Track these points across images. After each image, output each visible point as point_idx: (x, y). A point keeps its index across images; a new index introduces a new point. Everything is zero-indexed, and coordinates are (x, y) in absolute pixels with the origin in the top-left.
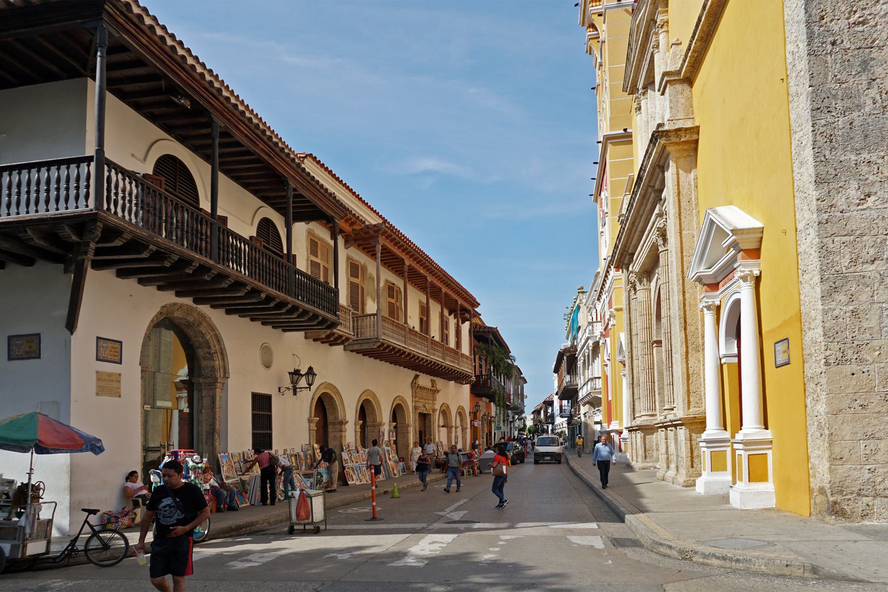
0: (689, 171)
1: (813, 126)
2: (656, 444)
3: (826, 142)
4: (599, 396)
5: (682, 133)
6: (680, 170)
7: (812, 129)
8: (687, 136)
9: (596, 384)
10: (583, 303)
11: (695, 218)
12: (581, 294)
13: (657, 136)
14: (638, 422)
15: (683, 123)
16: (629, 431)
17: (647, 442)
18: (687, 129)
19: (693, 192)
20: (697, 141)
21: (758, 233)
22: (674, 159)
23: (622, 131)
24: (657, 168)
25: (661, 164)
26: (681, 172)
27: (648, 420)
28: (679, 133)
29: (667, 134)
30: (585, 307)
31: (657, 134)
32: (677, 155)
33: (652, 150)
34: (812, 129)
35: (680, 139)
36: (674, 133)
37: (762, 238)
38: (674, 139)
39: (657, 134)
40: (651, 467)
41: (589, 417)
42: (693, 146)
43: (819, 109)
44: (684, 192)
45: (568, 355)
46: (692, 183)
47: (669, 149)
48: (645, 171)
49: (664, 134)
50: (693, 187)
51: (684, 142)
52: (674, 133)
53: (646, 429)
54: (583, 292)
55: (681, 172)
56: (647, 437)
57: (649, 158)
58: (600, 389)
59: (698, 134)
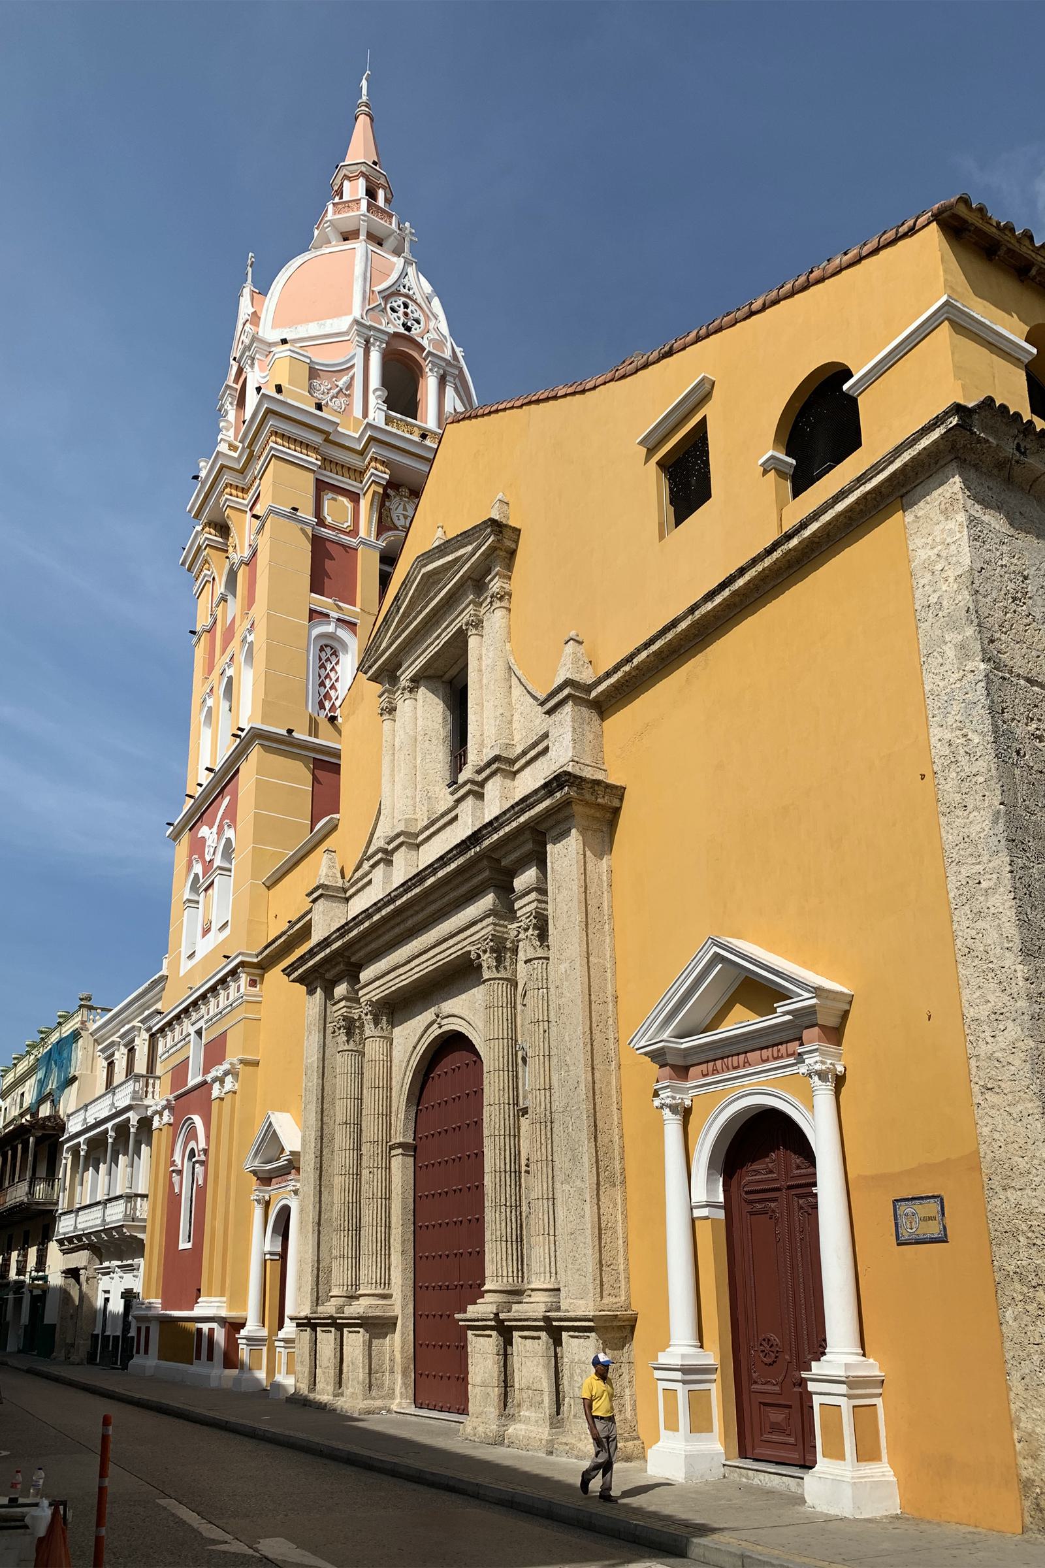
0: (600, 856)
1: (1010, 865)
2: (391, 1360)
3: (1025, 894)
4: (140, 1236)
6: (587, 849)
7: (1008, 868)
9: (135, 1209)
10: (87, 1030)
11: (608, 939)
12: (85, 1011)
13: (566, 781)
14: (328, 1309)
15: (592, 772)
16: (298, 1325)
17: (374, 1354)
19: (605, 893)
22: (580, 829)
24: (527, 832)
25: (541, 828)
26: (588, 853)
27: (377, 1306)
28: (596, 788)
30: (91, 1039)
32: (585, 824)
33: (540, 801)
34: (1008, 868)
35: (597, 798)
38: (588, 796)
39: (567, 778)
40: (381, 1409)
41: (88, 1279)
44: (592, 889)
45: (39, 1134)
46: (605, 878)
47: (577, 809)
48: (496, 830)
49: (577, 783)
50: (605, 884)
53: (374, 1325)
54: (90, 1008)
55: (588, 853)
56: (375, 1342)
57: (523, 811)
58: (144, 1220)
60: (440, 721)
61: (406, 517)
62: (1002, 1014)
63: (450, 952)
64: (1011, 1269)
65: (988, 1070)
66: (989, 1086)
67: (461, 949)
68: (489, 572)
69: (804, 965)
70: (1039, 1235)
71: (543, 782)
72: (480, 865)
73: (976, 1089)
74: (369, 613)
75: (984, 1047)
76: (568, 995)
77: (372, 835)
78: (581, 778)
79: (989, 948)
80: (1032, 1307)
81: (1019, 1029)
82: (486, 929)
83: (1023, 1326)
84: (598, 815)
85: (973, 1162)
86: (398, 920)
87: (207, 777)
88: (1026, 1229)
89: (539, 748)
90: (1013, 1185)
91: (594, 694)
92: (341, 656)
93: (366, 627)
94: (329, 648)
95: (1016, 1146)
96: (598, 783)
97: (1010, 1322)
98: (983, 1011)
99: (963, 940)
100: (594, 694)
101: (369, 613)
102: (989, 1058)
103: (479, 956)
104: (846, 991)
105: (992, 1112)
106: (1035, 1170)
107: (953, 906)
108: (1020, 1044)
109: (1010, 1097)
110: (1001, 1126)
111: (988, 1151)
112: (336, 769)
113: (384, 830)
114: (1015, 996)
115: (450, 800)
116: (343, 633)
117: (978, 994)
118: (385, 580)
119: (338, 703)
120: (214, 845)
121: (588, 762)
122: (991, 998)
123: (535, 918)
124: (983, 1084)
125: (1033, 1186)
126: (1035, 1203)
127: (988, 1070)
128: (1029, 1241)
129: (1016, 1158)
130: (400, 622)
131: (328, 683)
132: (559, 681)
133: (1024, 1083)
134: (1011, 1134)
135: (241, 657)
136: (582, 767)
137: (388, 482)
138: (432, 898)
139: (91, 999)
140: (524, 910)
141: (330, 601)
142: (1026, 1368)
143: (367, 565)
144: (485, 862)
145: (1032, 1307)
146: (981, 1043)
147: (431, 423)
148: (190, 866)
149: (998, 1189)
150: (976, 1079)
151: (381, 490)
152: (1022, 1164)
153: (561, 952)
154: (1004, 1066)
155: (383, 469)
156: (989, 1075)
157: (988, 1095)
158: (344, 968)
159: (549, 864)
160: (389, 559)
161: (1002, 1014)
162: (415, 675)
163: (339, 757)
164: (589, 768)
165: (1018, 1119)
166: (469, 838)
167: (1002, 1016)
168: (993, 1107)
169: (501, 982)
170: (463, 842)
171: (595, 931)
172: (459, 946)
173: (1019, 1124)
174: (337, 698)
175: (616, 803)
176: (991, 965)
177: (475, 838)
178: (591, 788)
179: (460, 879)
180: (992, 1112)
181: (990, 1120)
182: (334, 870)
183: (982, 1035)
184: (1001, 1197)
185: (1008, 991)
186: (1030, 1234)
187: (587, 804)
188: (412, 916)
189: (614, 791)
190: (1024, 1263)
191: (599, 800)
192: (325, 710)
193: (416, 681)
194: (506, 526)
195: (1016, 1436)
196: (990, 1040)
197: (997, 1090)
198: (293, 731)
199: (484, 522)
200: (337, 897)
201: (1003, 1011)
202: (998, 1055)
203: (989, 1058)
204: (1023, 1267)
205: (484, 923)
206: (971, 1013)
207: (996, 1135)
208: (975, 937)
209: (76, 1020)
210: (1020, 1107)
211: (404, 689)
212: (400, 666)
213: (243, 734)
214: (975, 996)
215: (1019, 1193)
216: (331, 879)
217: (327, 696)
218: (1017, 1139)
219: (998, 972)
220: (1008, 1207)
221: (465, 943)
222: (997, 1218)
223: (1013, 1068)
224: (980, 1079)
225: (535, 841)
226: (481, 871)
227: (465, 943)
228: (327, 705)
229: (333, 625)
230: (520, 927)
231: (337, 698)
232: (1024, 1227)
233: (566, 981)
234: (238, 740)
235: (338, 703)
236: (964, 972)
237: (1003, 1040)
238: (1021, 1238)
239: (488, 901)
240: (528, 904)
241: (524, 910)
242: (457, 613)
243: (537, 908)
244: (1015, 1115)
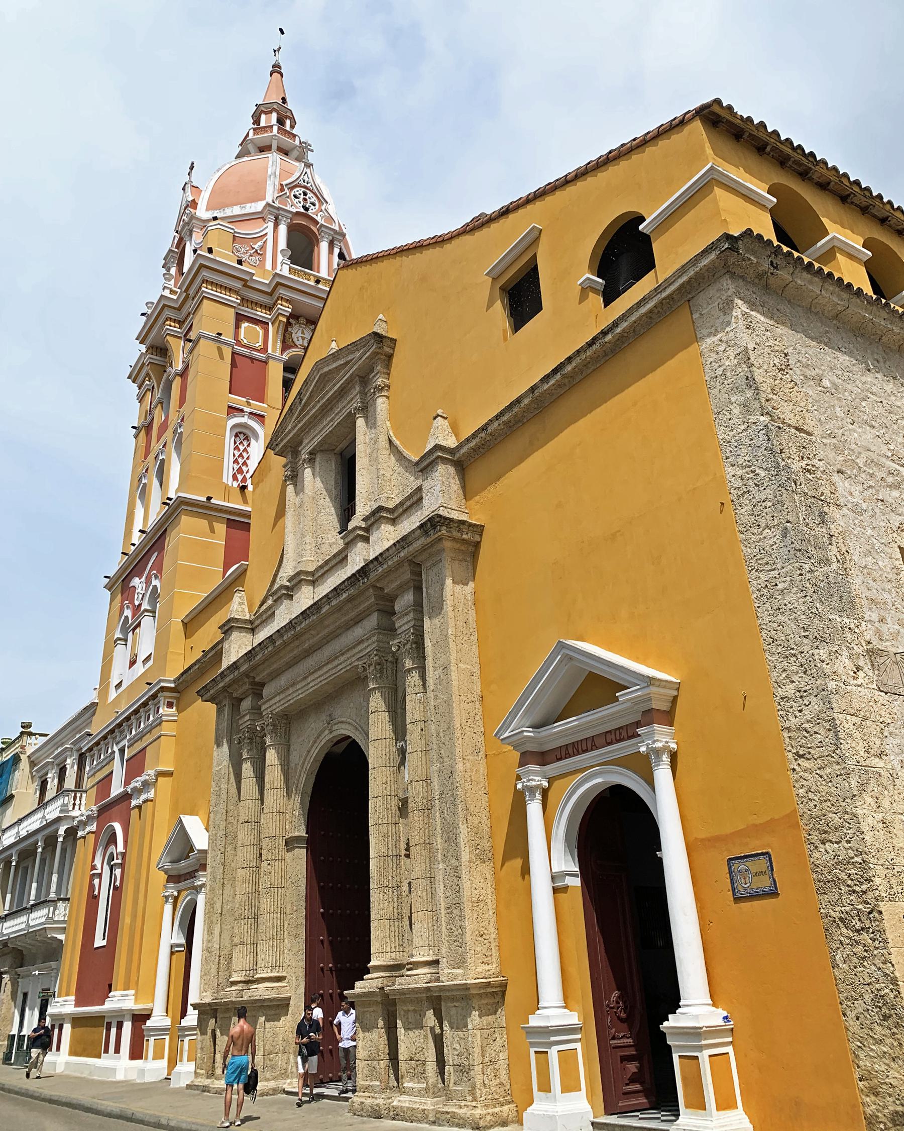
5: (464, 528)
8: (469, 534)
18: (470, 525)
20: (477, 545)
21: (670, 689)
23: (204, 499)
24: (406, 564)
29: (449, 524)
31: (438, 519)
36: (456, 525)
37: (675, 698)
38: (455, 534)
39: (438, 519)
42: (471, 549)
43: (800, 550)
51: (464, 540)
52: (456, 525)
59: (481, 536)
60: (333, 483)
61: (303, 339)
62: (805, 691)
63: (342, 666)
64: (836, 915)
65: (799, 740)
66: (801, 753)
67: (350, 664)
68: (372, 370)
69: (637, 660)
70: (857, 883)
71: (418, 524)
72: (367, 593)
73: (790, 755)
74: (274, 408)
75: (793, 720)
76: (442, 696)
77: (276, 576)
78: (449, 519)
79: (789, 637)
80: (859, 949)
81: (821, 703)
82: (370, 646)
83: (852, 967)
84: (463, 548)
85: (791, 820)
86: (297, 643)
87: (140, 537)
88: (845, 877)
89: (414, 500)
90: (830, 838)
91: (457, 456)
92: (253, 441)
93: (273, 418)
94: (242, 435)
95: (829, 804)
96: (463, 522)
97: (841, 965)
98: (790, 690)
99: (767, 632)
100: (457, 456)
101: (274, 408)
102: (798, 729)
103: (365, 669)
104: (674, 680)
105: (806, 775)
106: (847, 824)
107: (757, 605)
108: (823, 715)
109: (819, 761)
110: (814, 787)
111: (806, 811)
112: (246, 527)
113: (288, 570)
114: (815, 675)
115: (341, 544)
116: (253, 423)
117: (784, 675)
118: (287, 385)
119: (248, 476)
120: (143, 592)
121: (454, 507)
122: (795, 678)
123: (412, 634)
124: (795, 751)
125: (848, 838)
126: (851, 853)
127: (799, 740)
128: (849, 889)
129: (830, 815)
130: (302, 410)
131: (241, 461)
132: (429, 446)
133: (830, 749)
134: (824, 794)
135: (172, 447)
136: (450, 511)
137: (291, 314)
138: (326, 623)
139: (31, 726)
140: (404, 628)
141: (244, 400)
142: (860, 1006)
143: (275, 373)
144: (371, 590)
145: (859, 949)
146: (790, 716)
147: (324, 273)
148: (122, 611)
149: (818, 843)
150: (790, 748)
151: (285, 320)
152: (836, 820)
153: (436, 661)
154: (811, 735)
155: (287, 305)
156: (800, 743)
157: (800, 761)
158: (250, 687)
159: (424, 589)
160: (291, 368)
161: (805, 691)
162: (313, 449)
163: (249, 517)
164: (455, 512)
165: (829, 780)
166: (358, 571)
167: (805, 694)
168: (805, 771)
169: (384, 690)
170: (354, 575)
171: (463, 642)
172: (349, 662)
173: (830, 784)
174: (247, 472)
175: (477, 538)
176: (792, 652)
177: (363, 572)
178: (458, 527)
179: (350, 605)
180: (806, 775)
181: (804, 783)
182: (243, 606)
183: (791, 710)
184: (821, 850)
185: (809, 672)
186: (850, 882)
187: (454, 539)
188: (308, 639)
189: (475, 529)
190: (847, 909)
191: (464, 536)
192: (238, 481)
193: (313, 455)
194: (385, 337)
195: (856, 1076)
196: (798, 714)
197: (808, 756)
198: (211, 498)
199: (369, 335)
200: (244, 628)
201: (806, 688)
202: (806, 725)
203: (798, 729)
204: (847, 912)
205: (370, 642)
206: (781, 692)
207: (811, 795)
208: (778, 629)
209: (17, 746)
210: (828, 770)
211: (304, 460)
212: (301, 443)
213: (171, 503)
214: (781, 678)
215: (836, 845)
216: (240, 613)
217: (240, 471)
218: (829, 798)
219: (799, 656)
220: (828, 859)
221: (354, 659)
222: (819, 870)
223: (819, 736)
224: (792, 747)
225: (413, 573)
226: (368, 598)
227: (354, 659)
228: (240, 477)
229: (246, 417)
230: (400, 643)
231: (247, 472)
232: (843, 876)
233: (440, 685)
234: (167, 507)
235: (248, 476)
236: (770, 658)
237: (808, 714)
238: (842, 887)
239: (373, 621)
240: (406, 623)
241: (404, 628)
242: (346, 402)
243: (414, 625)
244: (826, 777)
